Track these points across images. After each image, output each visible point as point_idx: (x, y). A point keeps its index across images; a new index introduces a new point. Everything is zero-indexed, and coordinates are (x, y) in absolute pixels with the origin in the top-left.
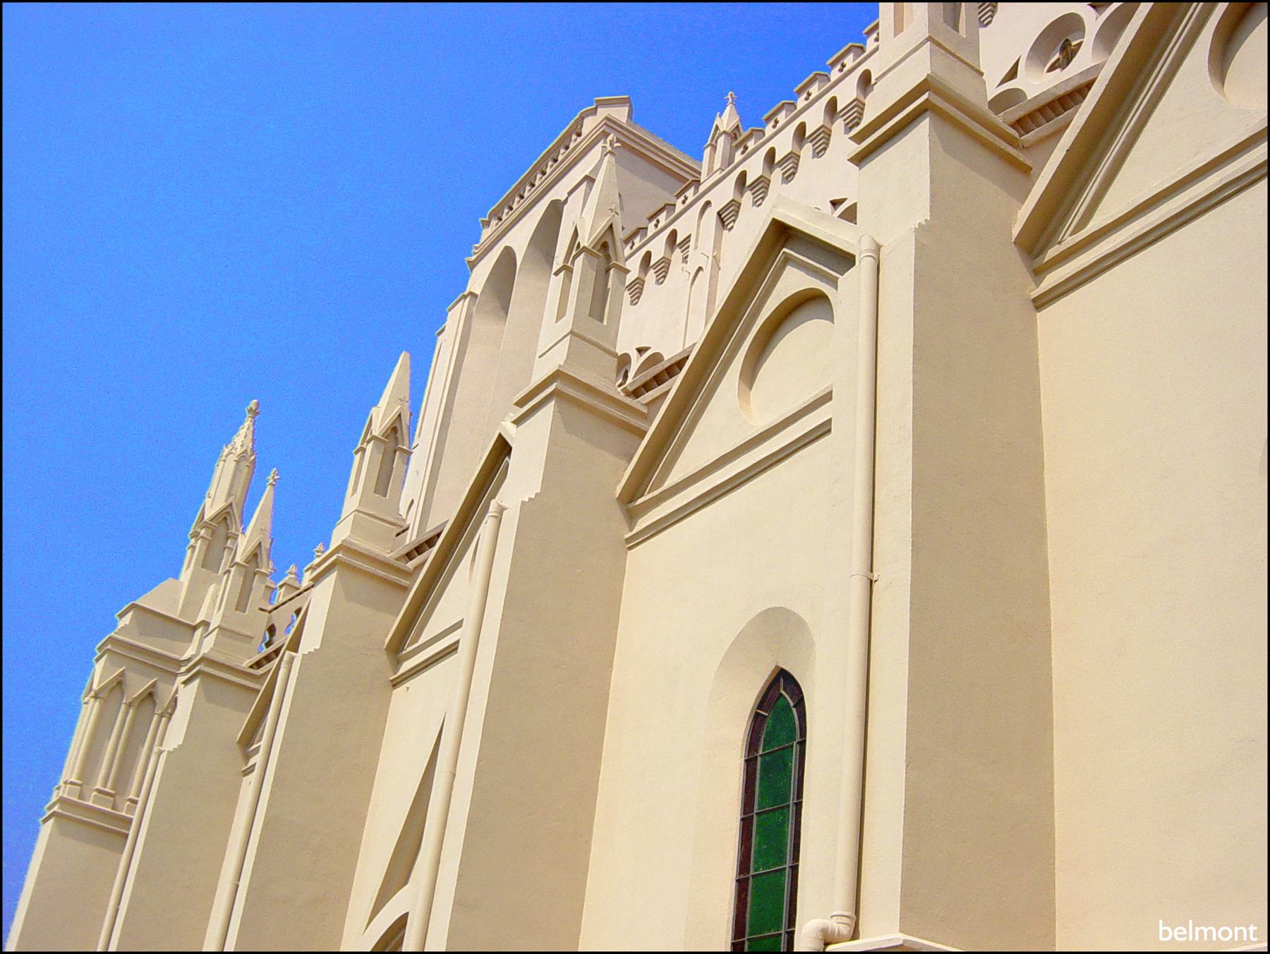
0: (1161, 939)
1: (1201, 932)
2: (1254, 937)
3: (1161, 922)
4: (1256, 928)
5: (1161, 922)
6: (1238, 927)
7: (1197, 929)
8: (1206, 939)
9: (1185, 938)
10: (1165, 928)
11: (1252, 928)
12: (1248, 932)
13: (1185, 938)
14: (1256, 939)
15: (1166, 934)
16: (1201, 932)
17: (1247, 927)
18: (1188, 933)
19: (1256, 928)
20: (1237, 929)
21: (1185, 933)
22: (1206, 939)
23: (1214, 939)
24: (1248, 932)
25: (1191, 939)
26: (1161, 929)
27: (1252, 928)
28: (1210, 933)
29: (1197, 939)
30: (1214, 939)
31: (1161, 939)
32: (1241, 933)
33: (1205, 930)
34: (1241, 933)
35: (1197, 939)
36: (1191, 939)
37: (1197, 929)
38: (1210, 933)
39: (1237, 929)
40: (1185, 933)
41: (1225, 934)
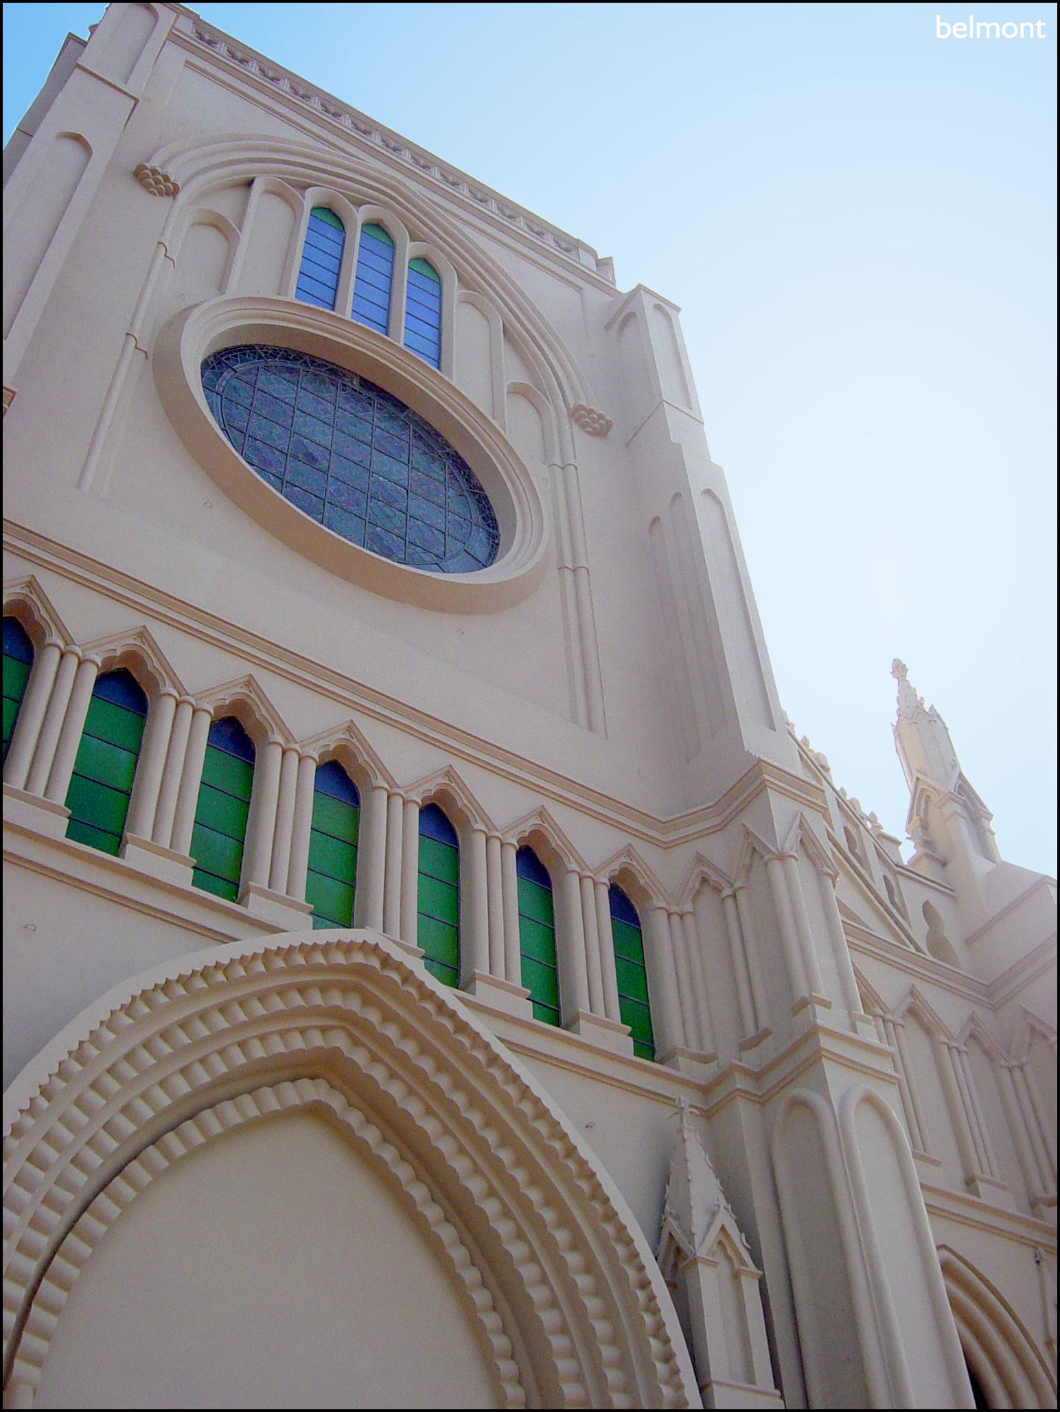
0: (939, 36)
1: (983, 29)
2: (1042, 34)
3: (938, 17)
4: (1044, 24)
5: (938, 17)
6: (1024, 23)
7: (979, 25)
8: (988, 36)
9: (965, 35)
10: (944, 24)
11: (1039, 24)
12: (1035, 28)
13: (965, 35)
14: (1044, 36)
15: (944, 30)
16: (983, 29)
17: (1034, 24)
18: (968, 28)
19: (1044, 24)
20: (1023, 25)
21: (965, 29)
22: (988, 36)
23: (998, 36)
24: (1035, 28)
25: (971, 36)
26: (939, 25)
27: (1039, 24)
28: (993, 29)
29: (978, 36)
30: (998, 36)
31: (939, 36)
32: (1027, 29)
33: (988, 26)
34: (1027, 29)
35: (978, 36)
36: (971, 36)
37: (979, 25)
38: (993, 29)
39: (1023, 25)
40: (965, 29)
41: (1010, 30)
